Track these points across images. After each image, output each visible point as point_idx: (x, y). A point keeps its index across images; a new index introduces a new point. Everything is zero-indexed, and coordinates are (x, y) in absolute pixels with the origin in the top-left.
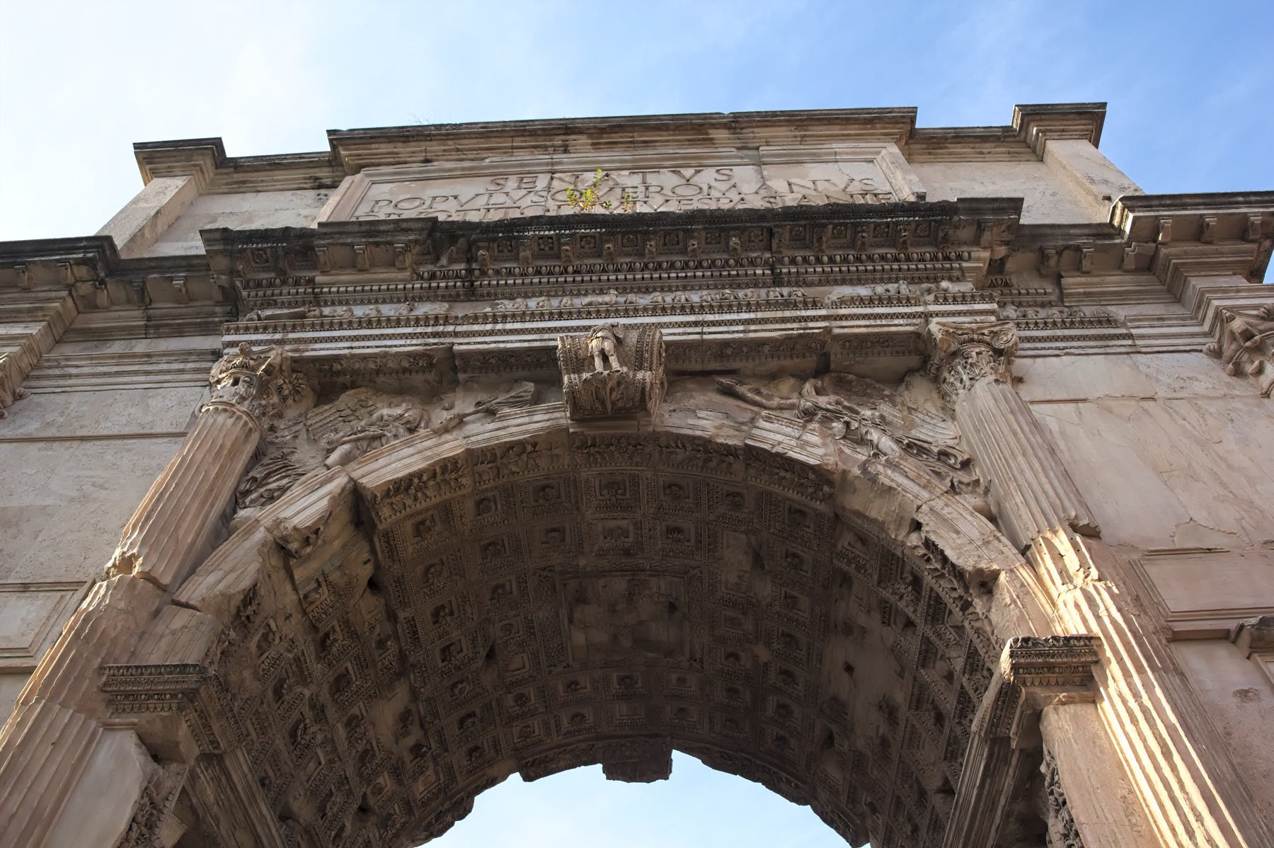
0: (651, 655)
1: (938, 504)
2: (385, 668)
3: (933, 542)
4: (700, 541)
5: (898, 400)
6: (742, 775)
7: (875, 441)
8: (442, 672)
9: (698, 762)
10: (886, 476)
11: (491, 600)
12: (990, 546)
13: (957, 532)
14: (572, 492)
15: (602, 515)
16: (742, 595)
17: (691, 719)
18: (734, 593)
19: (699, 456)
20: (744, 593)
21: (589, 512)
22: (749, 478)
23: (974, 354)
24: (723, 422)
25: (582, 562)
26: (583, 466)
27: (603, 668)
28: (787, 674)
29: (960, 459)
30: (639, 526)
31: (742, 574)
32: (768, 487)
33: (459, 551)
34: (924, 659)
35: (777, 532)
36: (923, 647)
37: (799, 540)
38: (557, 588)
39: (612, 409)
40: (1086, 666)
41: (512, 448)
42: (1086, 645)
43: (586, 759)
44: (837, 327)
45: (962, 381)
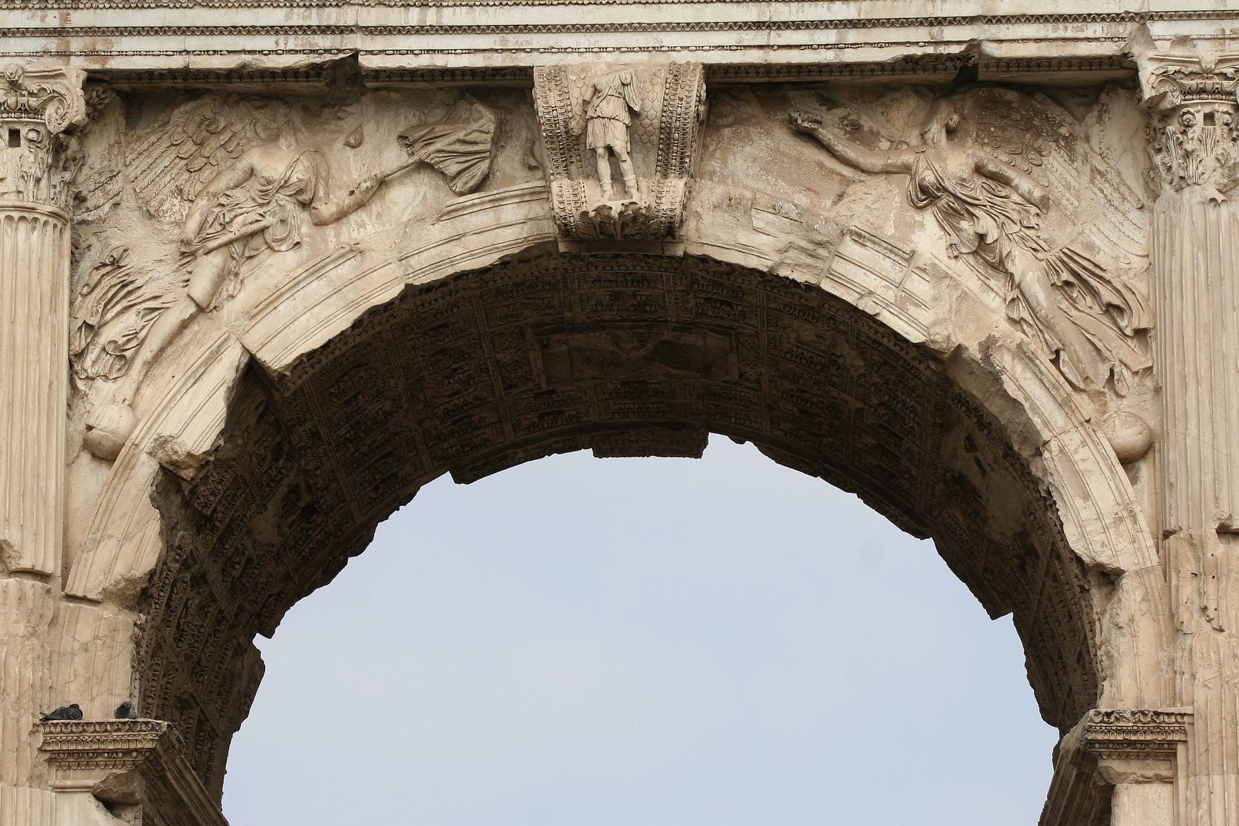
0: (674, 371)
1: (1073, 440)
2: (272, 481)
5: (1081, 147)
7: (1017, 279)
8: (346, 439)
10: (1013, 379)
12: (1122, 528)
13: (1086, 496)
23: (1200, 117)
24: (791, 238)
29: (1135, 325)
33: (385, 350)
35: (870, 342)
40: (1173, 744)
42: (1177, 722)
43: (561, 445)
44: (988, 40)
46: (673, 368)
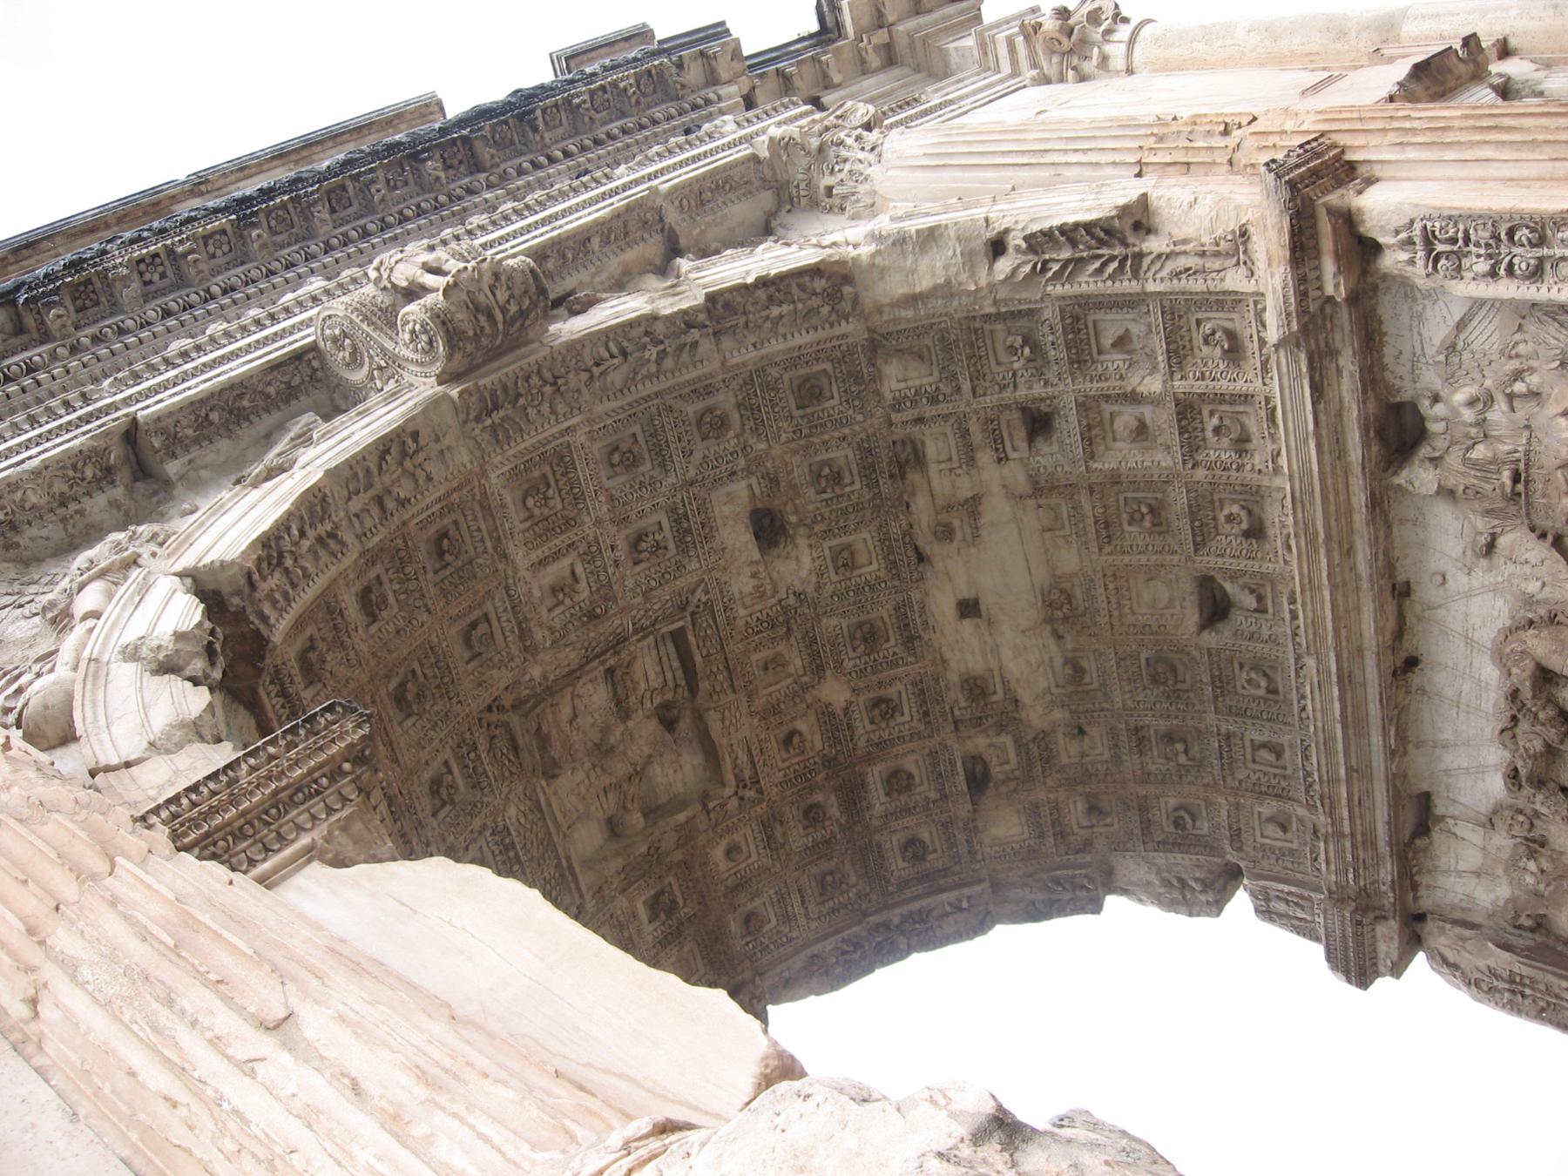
0: (681, 817)
3: (1041, 231)
4: (689, 531)
6: (883, 964)
9: (812, 998)
11: (434, 814)
13: (1058, 204)
14: (483, 527)
15: (539, 552)
16: (773, 601)
18: (758, 607)
19: (647, 354)
20: (773, 596)
21: (520, 555)
22: (728, 355)
25: (536, 672)
26: (493, 455)
27: (624, 890)
28: (884, 708)
30: (590, 554)
31: (754, 569)
32: (763, 352)
36: (1084, 423)
37: (829, 425)
39: (505, 322)
41: (387, 451)
45: (860, 161)
46: (680, 811)
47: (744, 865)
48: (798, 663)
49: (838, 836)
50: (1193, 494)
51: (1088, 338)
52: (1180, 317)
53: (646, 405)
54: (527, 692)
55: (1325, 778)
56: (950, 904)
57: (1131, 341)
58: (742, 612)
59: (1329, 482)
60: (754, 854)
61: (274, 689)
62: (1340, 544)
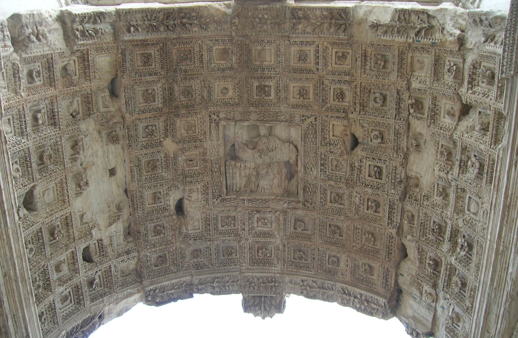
15: (271, 240)
17: (217, 47)
21: (278, 243)
30: (252, 229)
31: (189, 198)
34: (73, 257)
36: (76, 266)
38: (302, 192)
39: (261, 306)
43: (300, 12)
47: (222, 83)
48: (180, 159)
49: (180, 80)
50: (43, 254)
51: (73, 296)
52: (51, 321)
53: (220, 268)
54: (292, 203)
55: (5, 154)
56: (137, 30)
57: (61, 300)
58: (199, 187)
59: (18, 306)
60: (217, 86)
61: (389, 283)
62: (10, 278)
